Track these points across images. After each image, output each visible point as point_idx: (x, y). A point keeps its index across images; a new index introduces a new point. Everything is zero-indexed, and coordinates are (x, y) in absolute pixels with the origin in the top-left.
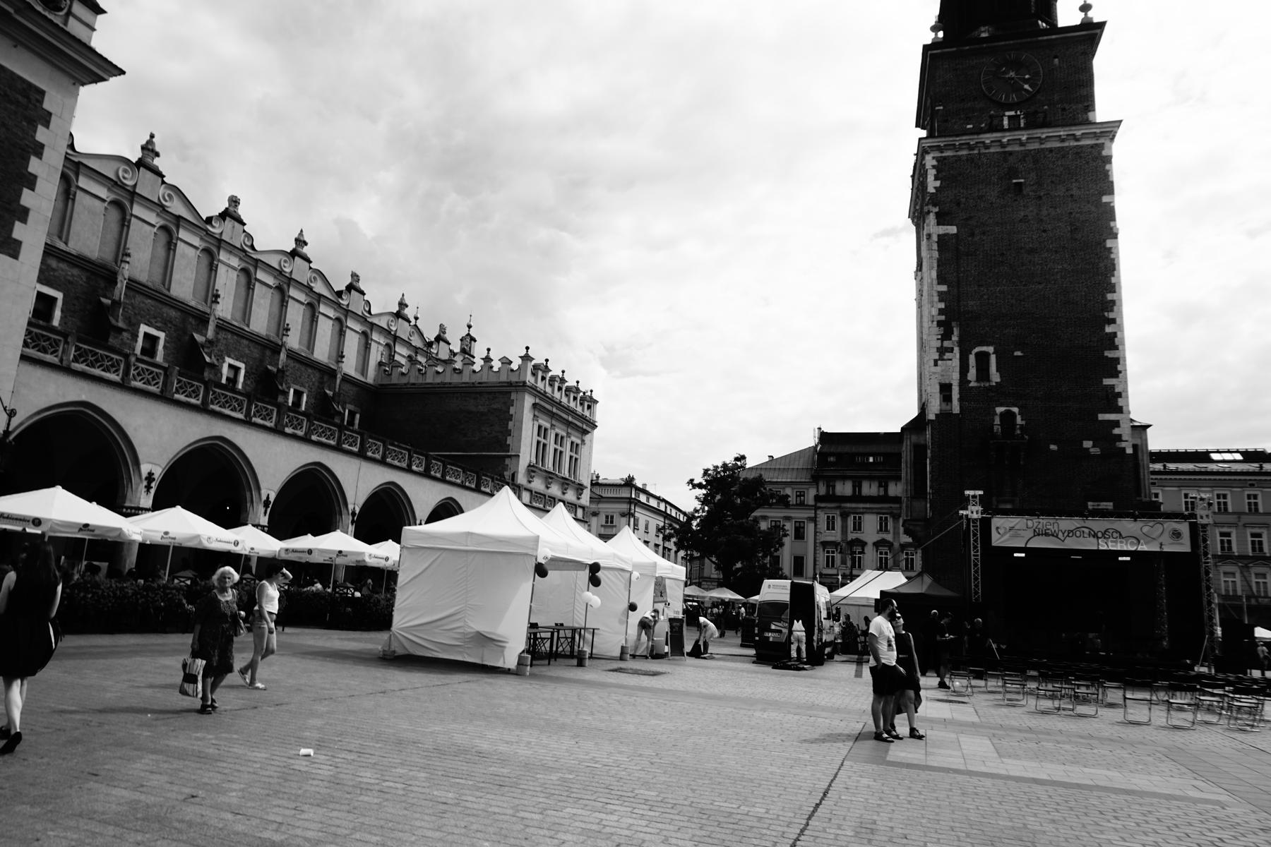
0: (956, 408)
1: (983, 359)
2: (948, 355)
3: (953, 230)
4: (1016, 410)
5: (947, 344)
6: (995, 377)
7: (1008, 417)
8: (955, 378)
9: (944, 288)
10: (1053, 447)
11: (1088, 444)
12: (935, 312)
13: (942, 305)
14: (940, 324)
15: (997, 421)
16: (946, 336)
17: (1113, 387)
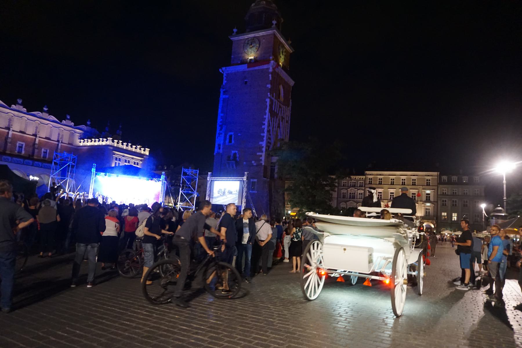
6: (233, 142)
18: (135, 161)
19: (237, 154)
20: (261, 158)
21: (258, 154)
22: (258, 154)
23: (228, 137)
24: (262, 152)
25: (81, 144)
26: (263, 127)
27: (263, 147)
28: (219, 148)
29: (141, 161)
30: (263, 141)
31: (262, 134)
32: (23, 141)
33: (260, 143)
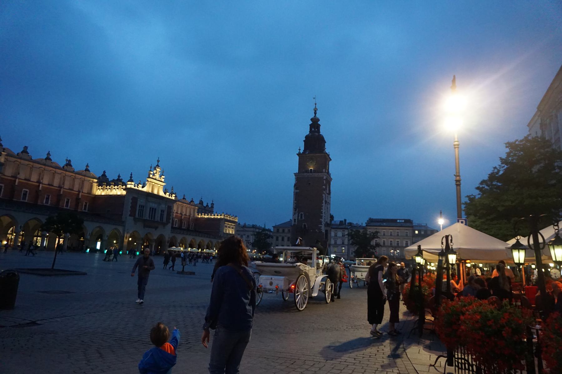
0: (296, 223)
1: (302, 215)
2: (296, 214)
3: (298, 191)
4: (306, 224)
5: (296, 212)
6: (303, 218)
7: (305, 225)
8: (296, 218)
9: (296, 202)
10: (311, 231)
11: (316, 230)
12: (294, 206)
13: (295, 205)
14: (295, 208)
15: (303, 226)
16: (295, 210)
17: (321, 221)
18: (233, 227)
19: (306, 225)
20: (321, 228)
21: (319, 226)
22: (319, 226)
23: (300, 215)
24: (322, 224)
25: (199, 217)
26: (322, 210)
27: (322, 222)
28: (295, 222)
29: (234, 226)
30: (322, 218)
31: (321, 215)
32: (177, 219)
33: (321, 220)
